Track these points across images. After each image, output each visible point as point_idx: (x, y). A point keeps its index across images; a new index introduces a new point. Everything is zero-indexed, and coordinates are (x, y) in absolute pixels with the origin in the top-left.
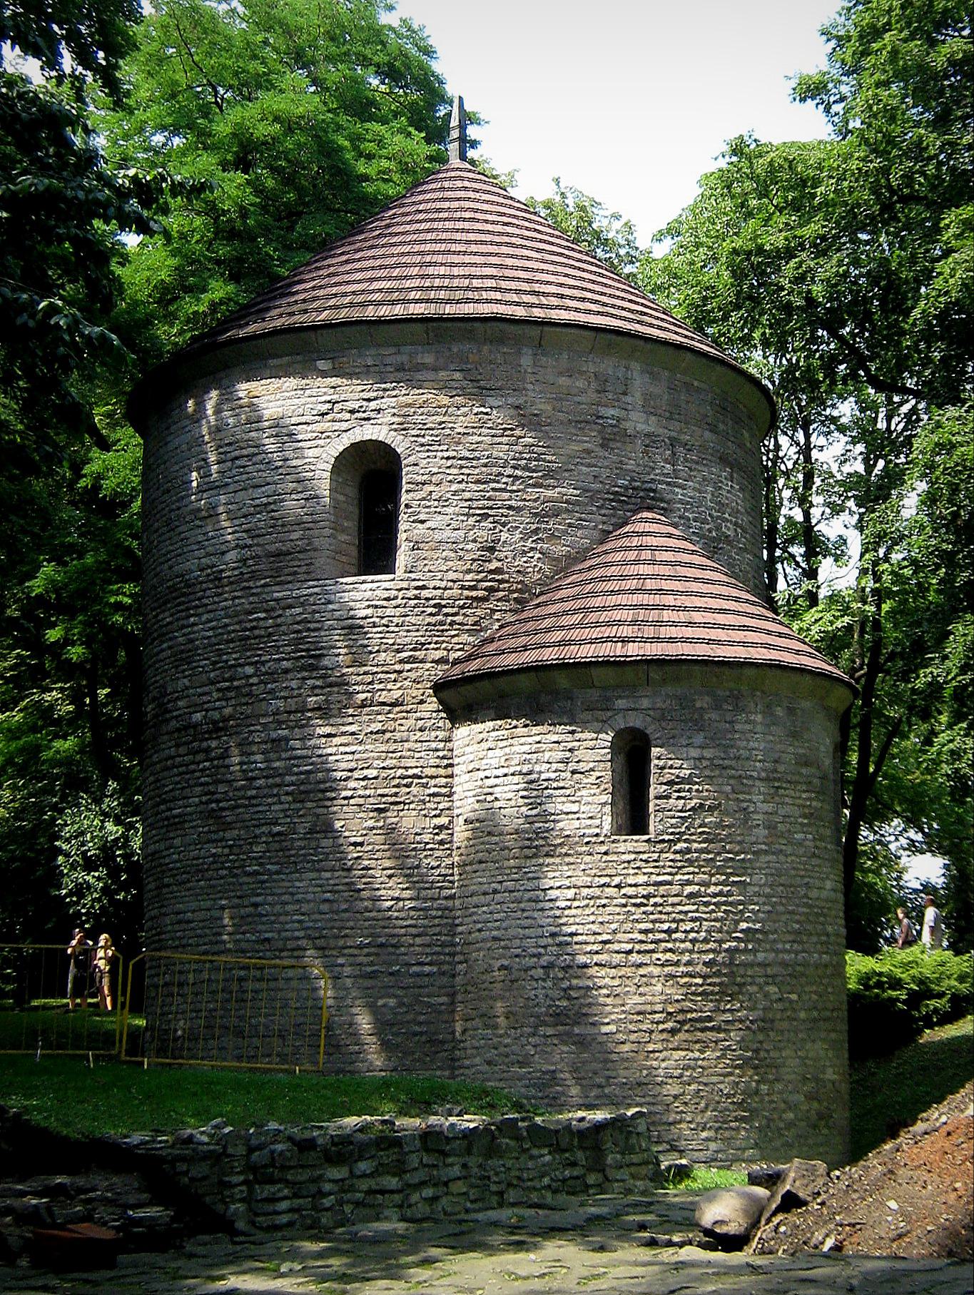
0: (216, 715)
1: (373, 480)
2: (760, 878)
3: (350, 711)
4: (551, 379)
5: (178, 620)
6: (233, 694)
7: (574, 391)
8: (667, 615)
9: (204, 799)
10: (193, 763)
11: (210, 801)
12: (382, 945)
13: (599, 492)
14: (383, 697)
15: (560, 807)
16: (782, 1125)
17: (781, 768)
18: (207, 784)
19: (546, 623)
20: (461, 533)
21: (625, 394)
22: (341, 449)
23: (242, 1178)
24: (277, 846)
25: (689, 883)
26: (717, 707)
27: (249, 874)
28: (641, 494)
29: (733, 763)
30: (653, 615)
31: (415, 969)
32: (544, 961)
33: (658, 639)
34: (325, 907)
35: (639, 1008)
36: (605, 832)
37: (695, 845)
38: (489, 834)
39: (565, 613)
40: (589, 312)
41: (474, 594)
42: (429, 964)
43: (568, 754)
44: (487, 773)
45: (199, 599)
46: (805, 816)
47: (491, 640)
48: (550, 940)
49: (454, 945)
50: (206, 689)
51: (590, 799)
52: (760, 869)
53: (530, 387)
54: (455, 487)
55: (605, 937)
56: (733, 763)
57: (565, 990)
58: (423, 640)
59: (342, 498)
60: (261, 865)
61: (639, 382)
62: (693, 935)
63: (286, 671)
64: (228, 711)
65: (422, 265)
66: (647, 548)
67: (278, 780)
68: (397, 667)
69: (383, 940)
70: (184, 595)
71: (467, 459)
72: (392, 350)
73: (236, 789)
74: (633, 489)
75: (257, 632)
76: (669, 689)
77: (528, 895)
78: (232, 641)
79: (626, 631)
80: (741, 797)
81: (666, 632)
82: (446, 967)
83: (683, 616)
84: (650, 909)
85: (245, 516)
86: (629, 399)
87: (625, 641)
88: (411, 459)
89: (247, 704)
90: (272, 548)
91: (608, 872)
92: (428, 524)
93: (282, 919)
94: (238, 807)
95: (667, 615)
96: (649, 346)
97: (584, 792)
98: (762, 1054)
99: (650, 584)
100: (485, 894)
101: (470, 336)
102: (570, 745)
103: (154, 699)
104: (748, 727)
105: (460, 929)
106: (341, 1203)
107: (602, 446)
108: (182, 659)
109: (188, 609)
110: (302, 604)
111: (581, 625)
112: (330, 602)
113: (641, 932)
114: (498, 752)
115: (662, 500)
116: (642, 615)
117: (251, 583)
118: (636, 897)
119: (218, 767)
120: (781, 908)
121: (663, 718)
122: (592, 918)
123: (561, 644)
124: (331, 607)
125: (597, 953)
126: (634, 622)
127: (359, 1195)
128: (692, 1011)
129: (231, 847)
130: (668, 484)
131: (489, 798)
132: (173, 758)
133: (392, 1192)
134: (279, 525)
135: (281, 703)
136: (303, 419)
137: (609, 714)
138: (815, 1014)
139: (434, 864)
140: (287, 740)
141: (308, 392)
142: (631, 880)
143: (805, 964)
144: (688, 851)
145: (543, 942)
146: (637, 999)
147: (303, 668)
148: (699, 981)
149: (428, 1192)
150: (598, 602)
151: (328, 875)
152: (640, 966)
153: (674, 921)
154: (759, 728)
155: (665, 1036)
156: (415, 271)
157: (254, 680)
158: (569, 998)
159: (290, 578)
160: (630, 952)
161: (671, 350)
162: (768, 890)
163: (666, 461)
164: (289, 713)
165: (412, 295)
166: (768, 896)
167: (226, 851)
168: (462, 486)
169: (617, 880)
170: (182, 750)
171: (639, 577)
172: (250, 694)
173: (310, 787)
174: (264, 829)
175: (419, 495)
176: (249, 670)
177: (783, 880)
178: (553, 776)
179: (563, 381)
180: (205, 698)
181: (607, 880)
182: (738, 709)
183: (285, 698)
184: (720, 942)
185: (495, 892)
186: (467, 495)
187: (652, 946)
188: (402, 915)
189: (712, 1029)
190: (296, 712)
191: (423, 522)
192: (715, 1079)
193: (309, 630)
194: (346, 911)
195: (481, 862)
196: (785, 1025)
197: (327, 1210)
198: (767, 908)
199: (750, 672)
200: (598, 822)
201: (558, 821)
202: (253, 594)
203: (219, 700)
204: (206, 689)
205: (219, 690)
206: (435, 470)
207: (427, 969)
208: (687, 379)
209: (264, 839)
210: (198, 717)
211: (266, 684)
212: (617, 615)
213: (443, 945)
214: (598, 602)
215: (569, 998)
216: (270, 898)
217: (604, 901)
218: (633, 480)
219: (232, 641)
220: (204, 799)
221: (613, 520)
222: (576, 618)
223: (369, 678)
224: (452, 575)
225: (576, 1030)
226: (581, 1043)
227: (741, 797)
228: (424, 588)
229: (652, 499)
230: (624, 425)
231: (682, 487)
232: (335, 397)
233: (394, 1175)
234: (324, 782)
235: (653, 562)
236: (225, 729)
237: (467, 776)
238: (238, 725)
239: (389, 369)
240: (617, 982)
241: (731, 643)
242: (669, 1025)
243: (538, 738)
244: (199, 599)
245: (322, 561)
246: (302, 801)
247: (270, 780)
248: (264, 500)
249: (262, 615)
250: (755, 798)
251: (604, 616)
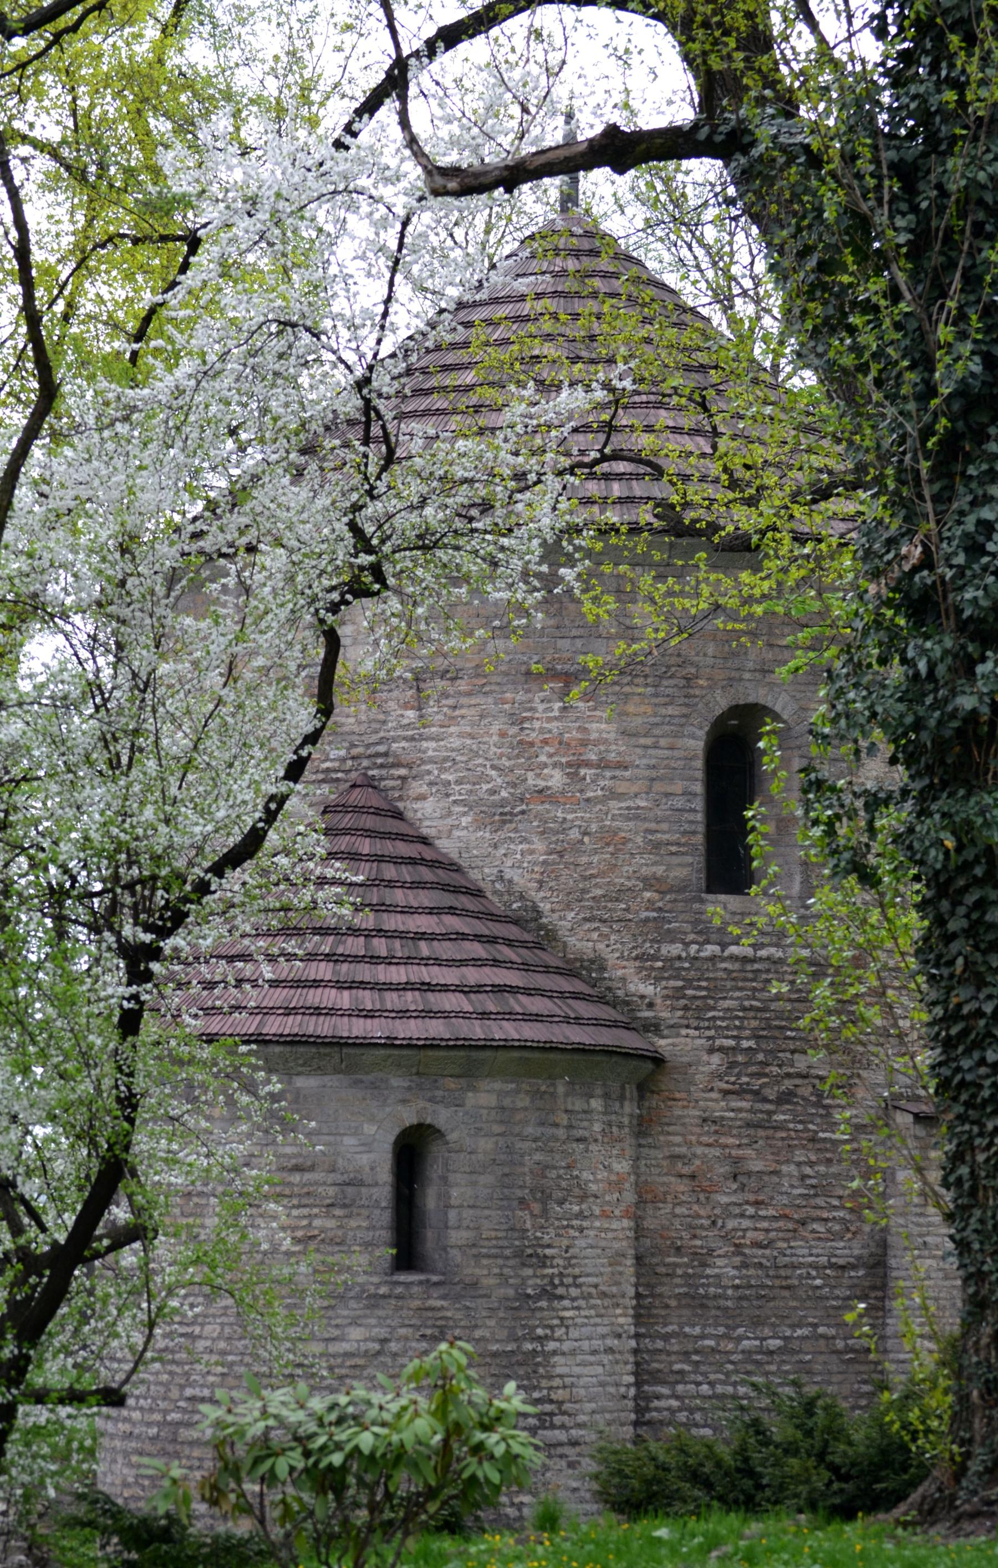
28: (365, 763)
52: (214, 1316)
74: (353, 758)
130: (412, 739)
162: (222, 1345)
163: (406, 706)
166: (223, 1353)
184: (165, 1412)
218: (353, 746)
229: (382, 766)
231: (437, 738)
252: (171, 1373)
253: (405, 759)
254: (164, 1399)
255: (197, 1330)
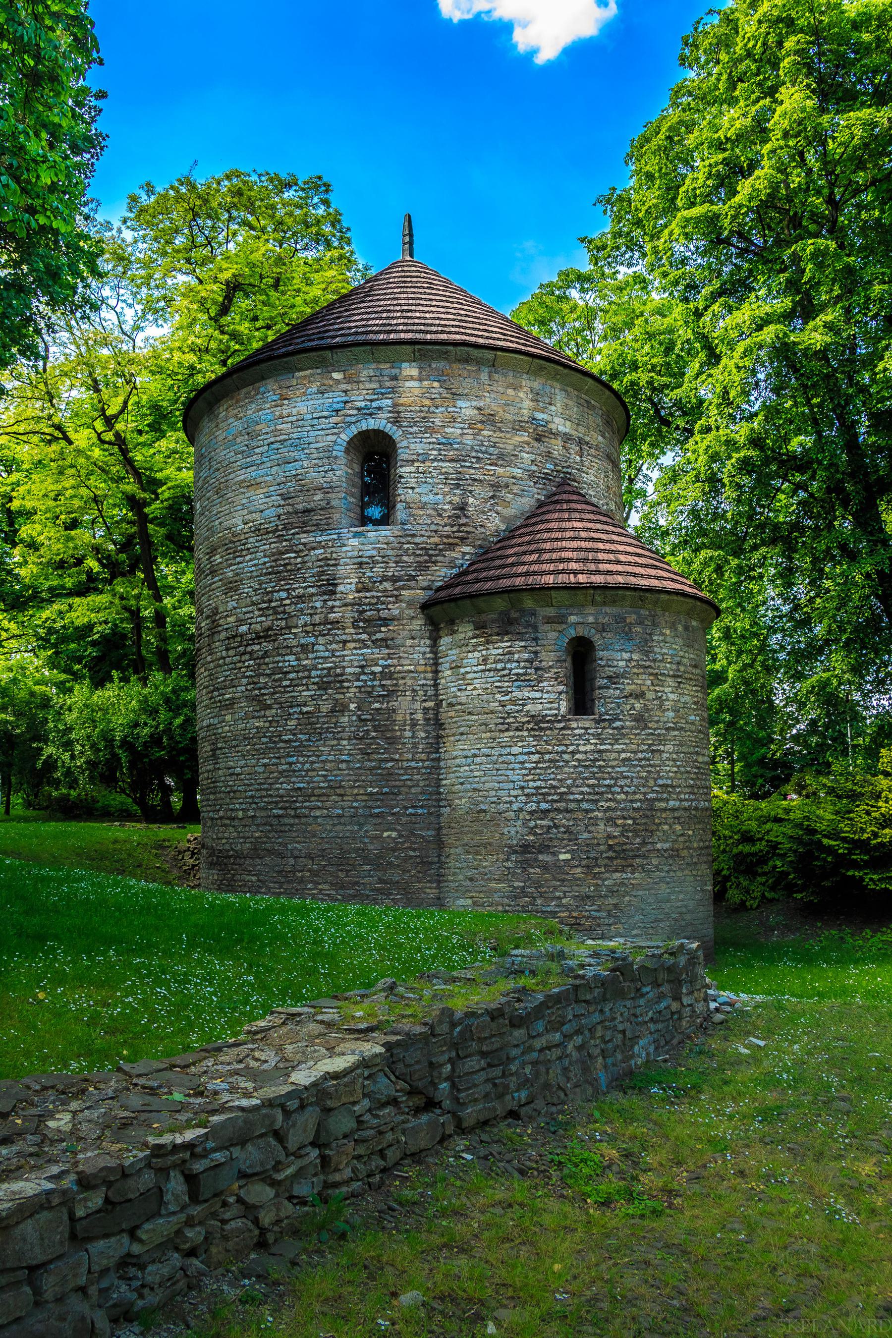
0: (258, 627)
1: (375, 457)
2: (669, 748)
3: (361, 624)
4: (502, 390)
5: (227, 560)
6: (271, 612)
7: (518, 400)
8: (601, 556)
9: (249, 687)
10: (240, 662)
11: (254, 689)
12: (386, 793)
13: (534, 471)
14: (384, 614)
15: (526, 694)
16: (683, 923)
17: (682, 668)
18: (251, 677)
19: (510, 560)
20: (440, 497)
21: (551, 404)
22: (351, 435)
23: (446, 1057)
24: (306, 721)
25: (623, 751)
26: (641, 623)
27: (286, 742)
29: (652, 664)
30: (590, 556)
31: (412, 811)
32: (515, 807)
33: (598, 572)
34: (343, 766)
35: (588, 842)
36: (562, 712)
37: (627, 723)
38: (470, 713)
39: (524, 553)
40: (526, 345)
41: (451, 541)
42: (422, 807)
43: (532, 656)
44: (468, 669)
45: (244, 544)
46: (695, 703)
47: (465, 573)
48: (520, 792)
49: (440, 793)
50: (250, 609)
51: (550, 689)
53: (487, 394)
54: (435, 464)
55: (563, 790)
56: (652, 664)
57: (532, 829)
58: (413, 573)
59: (350, 471)
60: (294, 735)
61: (560, 398)
62: (626, 789)
63: (312, 595)
64: (265, 625)
65: (402, 311)
66: (575, 510)
67: (306, 673)
68: (395, 593)
69: (385, 790)
70: (231, 542)
71: (443, 444)
72: (388, 365)
73: (274, 680)
75: (289, 567)
76: (608, 610)
77: (501, 759)
78: (270, 574)
79: (574, 566)
80: (658, 688)
81: (603, 567)
82: (432, 810)
83: (611, 557)
84: (596, 770)
85: (279, 484)
86: (553, 408)
87: (576, 573)
88: (404, 443)
89: (281, 619)
90: (300, 507)
91: (564, 742)
92: (417, 490)
93: (310, 774)
94: (276, 693)
95: (601, 556)
96: (566, 371)
97: (545, 684)
98: (672, 874)
99: (583, 534)
100: (466, 757)
101: (445, 356)
102: (534, 649)
103: (208, 617)
104: (661, 638)
105: (444, 782)
106: (523, 1065)
107: (536, 440)
108: (231, 588)
109: (235, 552)
110: (324, 547)
111: (538, 562)
112: (344, 545)
113: (588, 786)
114: (477, 654)
115: (574, 481)
116: (582, 555)
117: (284, 533)
118: (585, 761)
119: (259, 665)
120: (683, 769)
121: (604, 630)
122: (552, 776)
123: (527, 574)
124: (344, 549)
125: (556, 801)
126: (578, 561)
127: (535, 1055)
128: (625, 844)
129: (270, 722)
131: (469, 688)
132: (224, 658)
133: (557, 1046)
134: (304, 490)
135: (308, 618)
136: (323, 414)
137: (564, 626)
138: (701, 844)
139: (423, 735)
140: (313, 645)
141: (326, 395)
142: (581, 748)
143: (696, 809)
144: (623, 727)
145: (513, 793)
146: (586, 835)
147: (325, 593)
148: (630, 822)
149: (578, 1040)
150: (548, 546)
151: (345, 742)
152: (587, 811)
153: (612, 778)
154: (668, 639)
155: (606, 861)
156: (399, 314)
157: (288, 602)
158: (535, 834)
159: (313, 528)
160: (582, 801)
161: (579, 376)
162: (675, 756)
163: (576, 453)
164: (314, 625)
165: (401, 327)
166: (675, 760)
167: (267, 725)
168: (440, 464)
169: (571, 748)
170: (231, 653)
171: (574, 529)
172: (284, 612)
173: (330, 679)
174: (295, 709)
175: (408, 469)
176: (283, 595)
177: (684, 749)
178: (521, 671)
179: (510, 392)
180: (249, 615)
181: (564, 748)
182: (654, 624)
183: (311, 615)
184: (645, 794)
185: (475, 756)
186: (444, 470)
187: (597, 797)
188: (402, 772)
189: (639, 856)
190: (320, 624)
191: (412, 488)
192: (640, 893)
193: (328, 565)
194: (358, 768)
195: (462, 734)
196: (685, 853)
197: (512, 1075)
198: (675, 769)
199: (664, 597)
200: (556, 705)
201: (524, 705)
202: (286, 540)
203: (261, 616)
204: (250, 609)
205: (260, 609)
206: (421, 452)
207: (420, 811)
208: (588, 398)
209: (296, 716)
210: (243, 629)
211: (296, 604)
212: (564, 554)
213: (430, 794)
214: (548, 546)
215: (535, 834)
216: (301, 759)
217: (561, 764)
218: (556, 465)
219: (270, 574)
220: (249, 687)
221: (545, 492)
222: (534, 557)
223: (375, 600)
224: (433, 527)
225: (541, 857)
226: (545, 867)
227: (658, 688)
228: (414, 536)
230: (553, 426)
232: (347, 398)
233: (557, 1030)
234: (342, 675)
235: (581, 520)
236: (265, 637)
237: (449, 672)
238: (276, 635)
239: (386, 378)
240: (571, 823)
241: (650, 577)
242: (611, 854)
243: (509, 644)
244: (244, 544)
245: (338, 516)
246: (325, 689)
247: (300, 674)
248: (294, 472)
249: (293, 555)
250: (666, 690)
251: (554, 556)
252: (648, 772)
253: (578, 479)
254: (644, 786)
255: (662, 748)
